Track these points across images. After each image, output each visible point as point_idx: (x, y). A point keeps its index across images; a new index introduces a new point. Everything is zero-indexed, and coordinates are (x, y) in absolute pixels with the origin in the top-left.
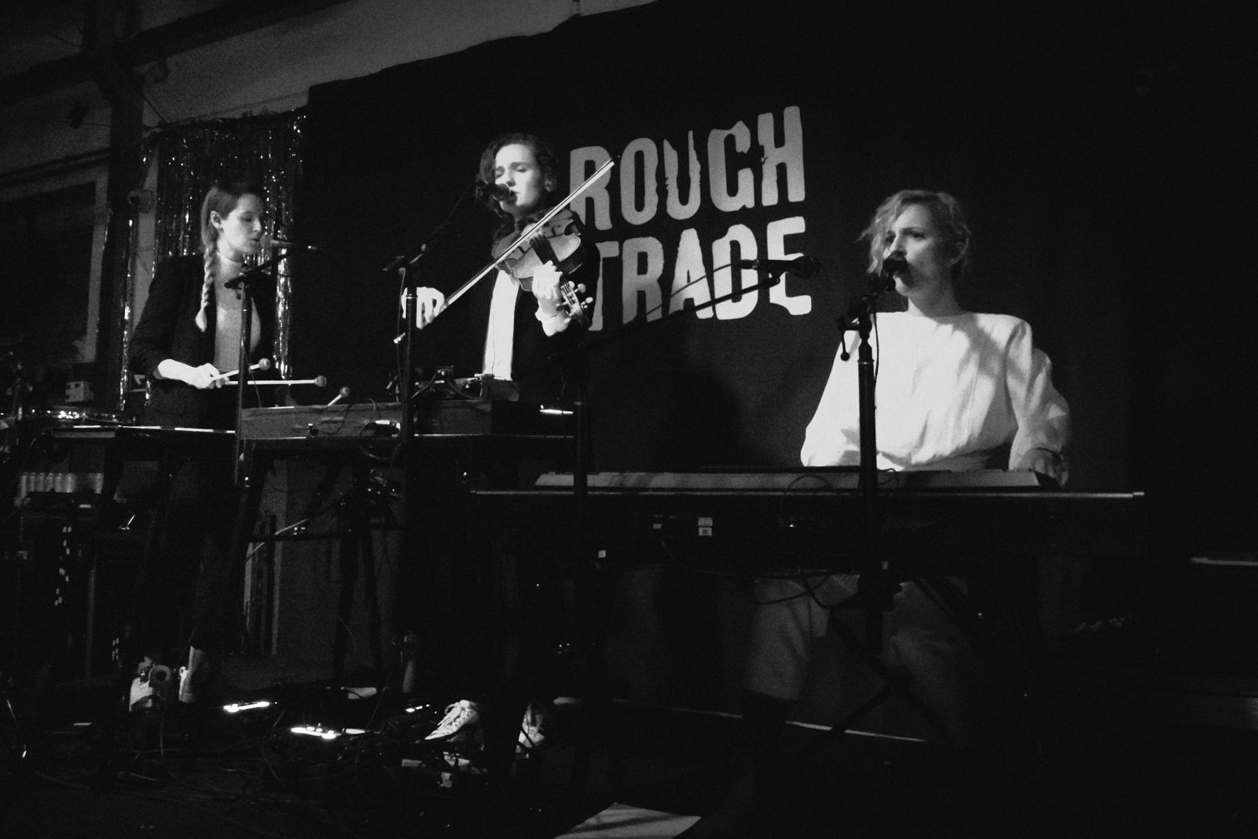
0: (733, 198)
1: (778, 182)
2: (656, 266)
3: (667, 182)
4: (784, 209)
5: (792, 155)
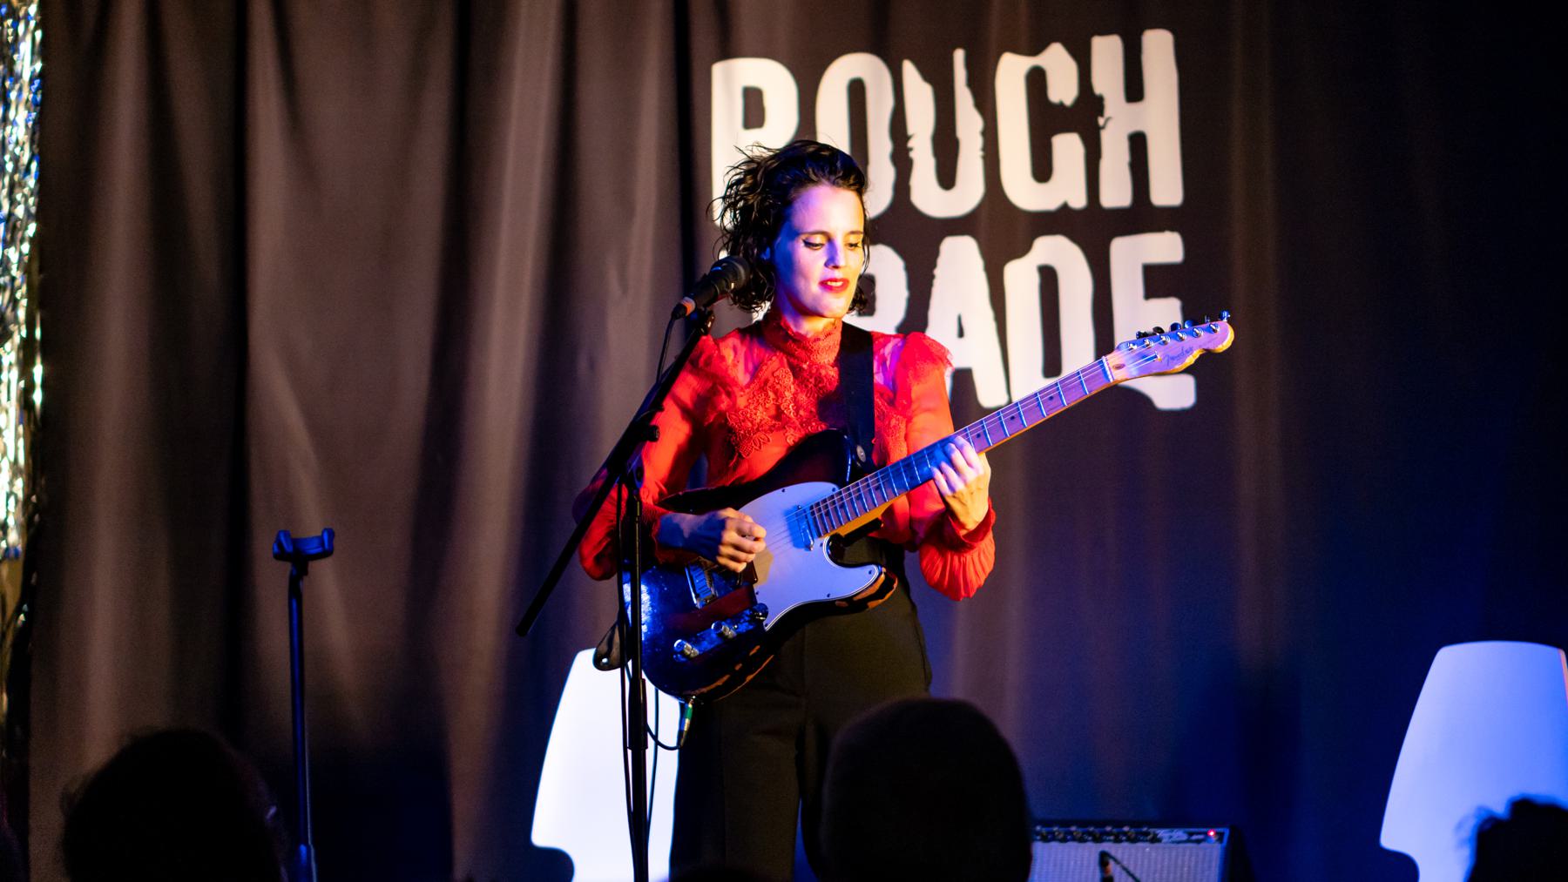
3: (911, 144)
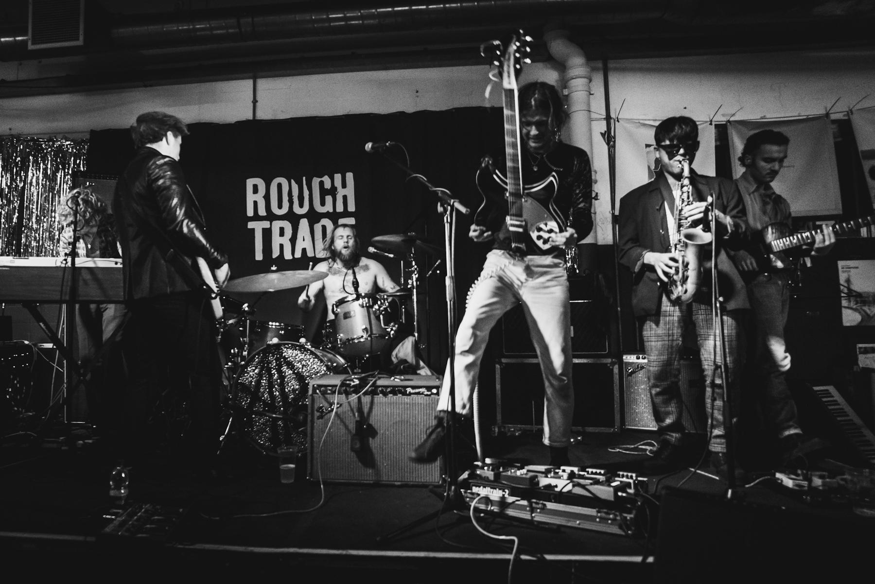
0: (325, 207)
1: (343, 202)
2: (289, 232)
4: (346, 214)
5: (350, 191)
